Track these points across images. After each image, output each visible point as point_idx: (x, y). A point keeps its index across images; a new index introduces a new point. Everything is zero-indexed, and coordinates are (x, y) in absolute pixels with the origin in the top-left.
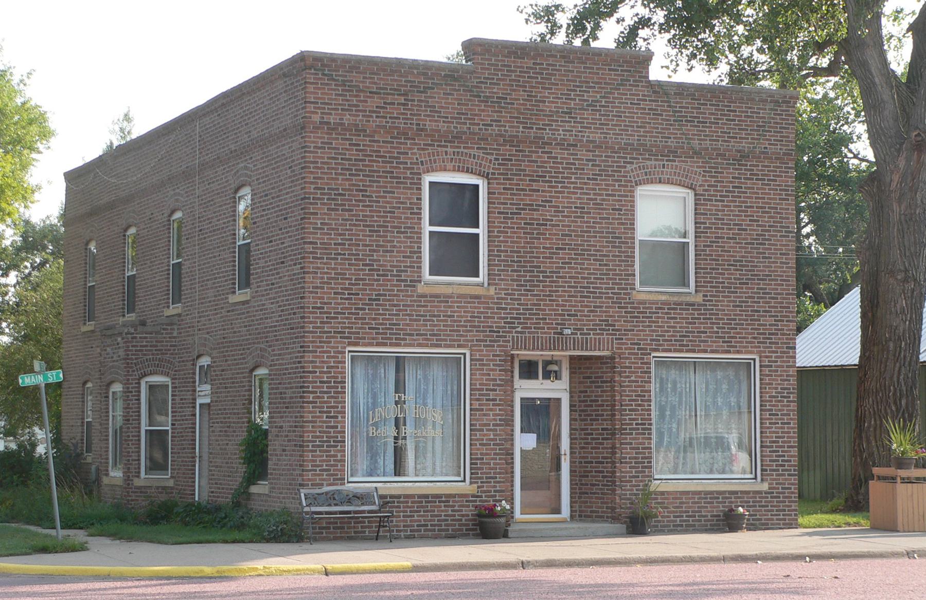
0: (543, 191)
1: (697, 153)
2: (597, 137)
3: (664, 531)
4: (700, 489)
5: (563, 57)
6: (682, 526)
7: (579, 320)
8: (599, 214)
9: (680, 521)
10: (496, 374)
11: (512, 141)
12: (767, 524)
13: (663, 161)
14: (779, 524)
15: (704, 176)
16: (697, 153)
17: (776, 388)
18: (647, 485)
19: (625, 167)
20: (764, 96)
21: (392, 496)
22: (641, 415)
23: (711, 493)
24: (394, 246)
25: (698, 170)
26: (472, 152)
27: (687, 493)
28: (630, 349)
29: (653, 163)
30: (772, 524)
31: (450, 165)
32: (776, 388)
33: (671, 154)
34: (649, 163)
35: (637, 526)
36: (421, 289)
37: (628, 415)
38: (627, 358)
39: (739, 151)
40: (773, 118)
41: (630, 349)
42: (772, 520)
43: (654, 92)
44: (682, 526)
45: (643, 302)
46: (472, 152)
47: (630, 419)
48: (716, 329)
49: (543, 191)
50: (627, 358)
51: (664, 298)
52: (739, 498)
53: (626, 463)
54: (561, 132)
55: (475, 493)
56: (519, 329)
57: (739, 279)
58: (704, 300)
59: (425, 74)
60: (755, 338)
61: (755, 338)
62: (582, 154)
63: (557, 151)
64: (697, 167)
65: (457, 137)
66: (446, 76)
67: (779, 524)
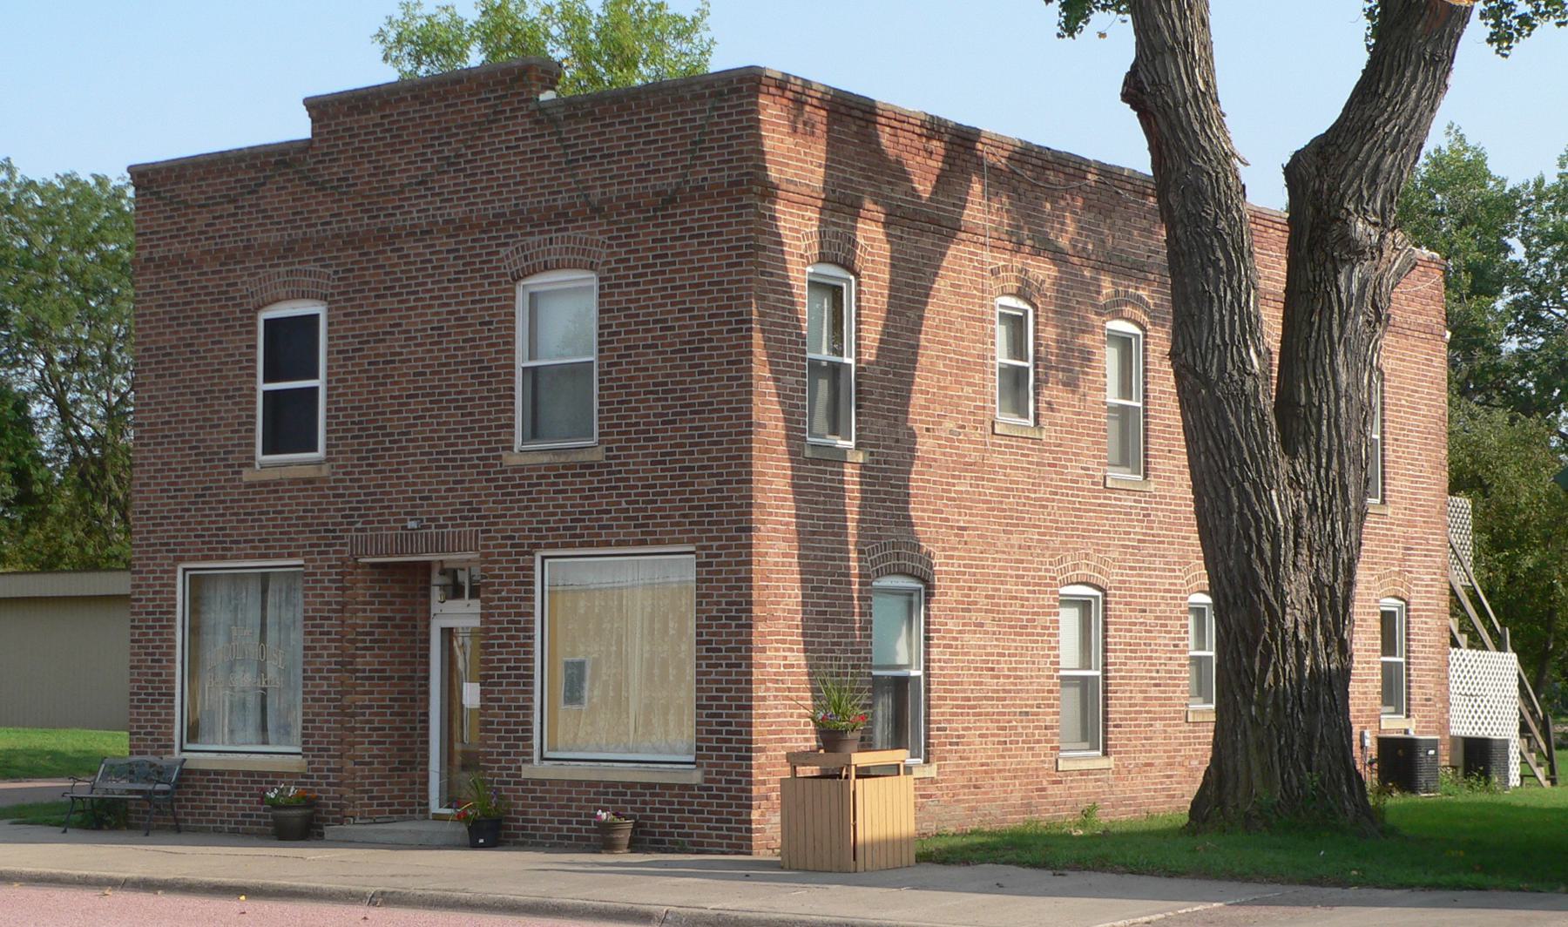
0: (392, 310)
1: (597, 210)
2: (457, 212)
3: (543, 845)
4: (594, 777)
5: (415, 98)
6: (569, 838)
7: (434, 505)
8: (462, 333)
9: (569, 830)
10: (332, 595)
11: (352, 240)
12: (702, 844)
13: (549, 228)
14: (721, 845)
15: (610, 246)
16: (597, 210)
17: (718, 603)
18: (519, 769)
19: (497, 253)
20: (697, 88)
21: (217, 773)
22: (514, 653)
23: (614, 784)
24: (221, 419)
25: (601, 238)
26: (308, 267)
27: (578, 783)
28: (501, 546)
29: (537, 238)
30: (710, 844)
31: (282, 292)
32: (718, 603)
33: (559, 218)
34: (530, 239)
35: (490, 830)
36: (247, 475)
37: (495, 653)
38: (496, 562)
39: (657, 194)
40: (717, 124)
41: (501, 546)
42: (709, 836)
43: (537, 122)
44: (569, 838)
45: (518, 469)
46: (308, 267)
47: (500, 661)
48: (624, 505)
49: (392, 310)
50: (496, 562)
51: (545, 459)
52: (657, 795)
53: (492, 731)
54: (415, 215)
55: (304, 770)
56: (359, 525)
57: (661, 415)
58: (608, 458)
59: (254, 166)
60: (684, 516)
61: (684, 516)
62: (443, 243)
63: (409, 247)
64: (601, 233)
65: (289, 250)
66: (276, 163)
67: (721, 845)
